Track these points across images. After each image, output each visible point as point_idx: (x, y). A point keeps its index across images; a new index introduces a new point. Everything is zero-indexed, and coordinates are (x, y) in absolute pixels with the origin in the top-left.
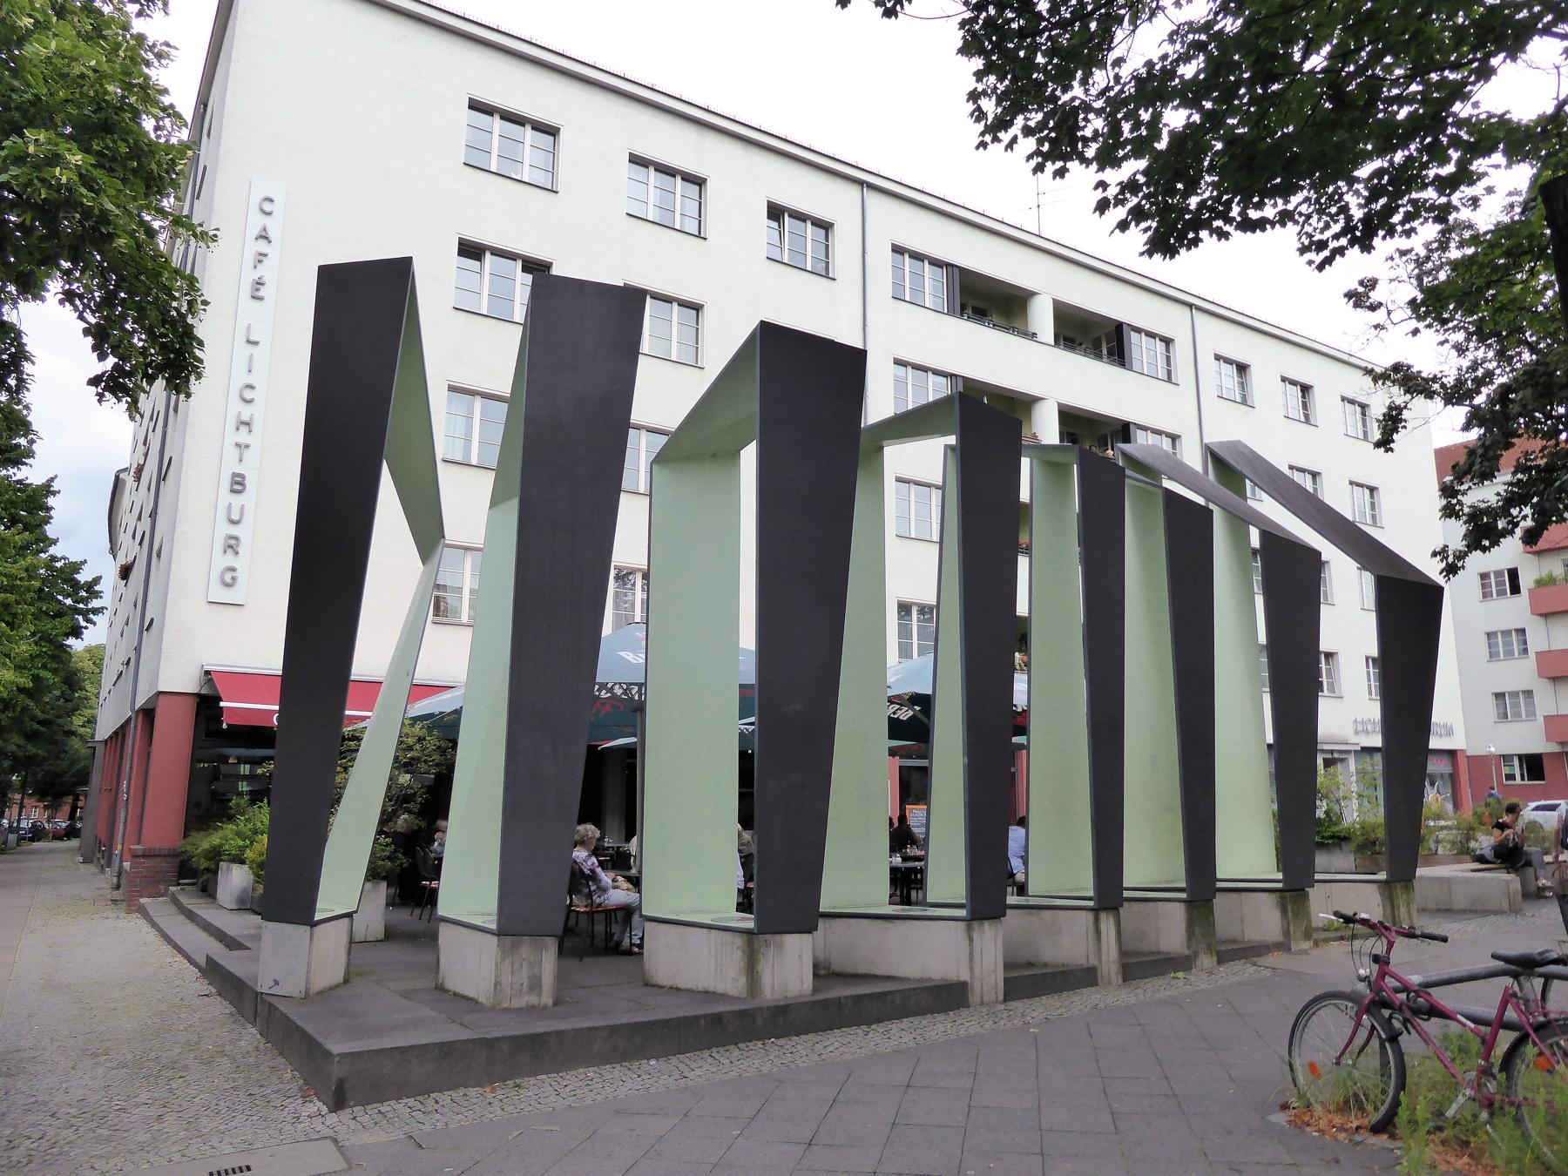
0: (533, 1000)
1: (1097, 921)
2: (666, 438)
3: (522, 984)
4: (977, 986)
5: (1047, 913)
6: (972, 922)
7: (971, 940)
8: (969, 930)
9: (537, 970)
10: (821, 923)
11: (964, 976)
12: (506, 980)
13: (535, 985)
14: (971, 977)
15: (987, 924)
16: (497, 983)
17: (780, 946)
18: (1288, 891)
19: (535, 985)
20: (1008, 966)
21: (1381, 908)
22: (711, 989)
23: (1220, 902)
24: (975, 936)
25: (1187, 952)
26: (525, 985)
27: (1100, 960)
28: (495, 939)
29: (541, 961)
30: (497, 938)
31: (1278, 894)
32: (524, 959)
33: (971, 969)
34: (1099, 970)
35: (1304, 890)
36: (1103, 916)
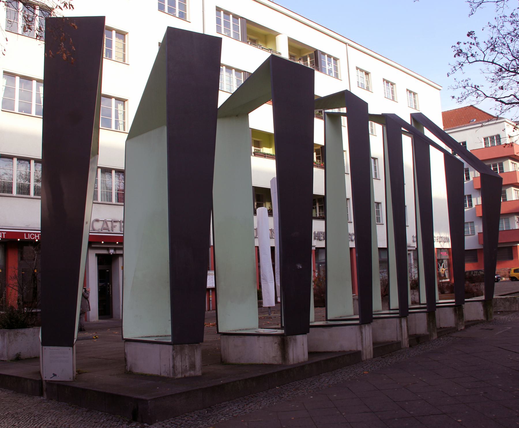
0: (192, 373)
1: (401, 322)
2: (410, 124)
3: (186, 366)
4: (364, 352)
5: (380, 320)
6: (362, 325)
7: (362, 333)
8: (361, 328)
9: (193, 359)
10: (311, 329)
11: (360, 348)
12: (178, 364)
13: (193, 366)
14: (362, 349)
15: (367, 326)
16: (174, 367)
17: (295, 340)
18: (457, 306)
19: (193, 366)
20: (374, 344)
21: (483, 311)
22: (271, 363)
23: (437, 311)
24: (363, 331)
25: (428, 333)
26: (188, 366)
27: (402, 338)
28: (171, 347)
29: (195, 354)
30: (441, 326)
31: (454, 307)
32: (186, 355)
33: (362, 347)
34: (401, 343)
35: (461, 305)
36: (403, 319)
